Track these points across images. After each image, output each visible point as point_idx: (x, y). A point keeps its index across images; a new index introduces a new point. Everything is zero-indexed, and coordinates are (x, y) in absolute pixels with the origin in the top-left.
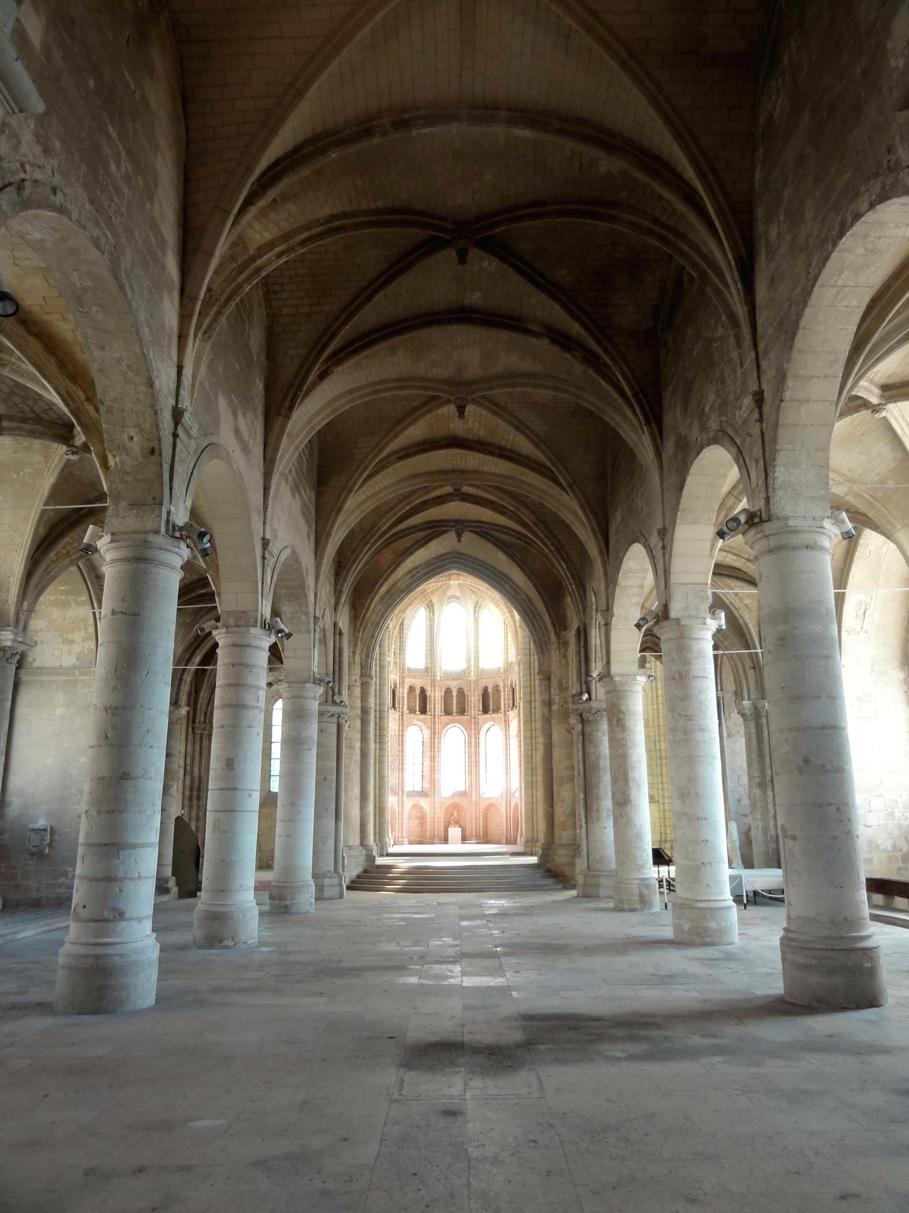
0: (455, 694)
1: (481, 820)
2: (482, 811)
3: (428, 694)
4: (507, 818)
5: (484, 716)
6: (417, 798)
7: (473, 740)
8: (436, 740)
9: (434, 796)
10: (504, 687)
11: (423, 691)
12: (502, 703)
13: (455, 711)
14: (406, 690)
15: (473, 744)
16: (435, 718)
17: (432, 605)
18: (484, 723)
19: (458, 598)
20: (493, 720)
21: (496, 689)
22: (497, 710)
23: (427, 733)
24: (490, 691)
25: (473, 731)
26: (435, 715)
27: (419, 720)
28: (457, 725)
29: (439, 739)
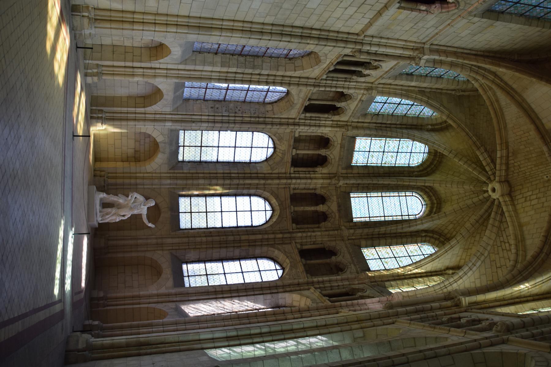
0: (321, 208)
1: (134, 254)
2: (148, 255)
3: (319, 169)
4: (139, 297)
5: (296, 251)
6: (167, 151)
7: (259, 237)
8: (256, 181)
9: (170, 178)
10: (347, 279)
11: (322, 161)
12: (326, 278)
13: (297, 209)
14: (326, 131)
15: (252, 237)
16: (286, 178)
17: (428, 174)
18: (285, 253)
19: (439, 209)
20: (293, 266)
21: (339, 269)
22: (310, 271)
23: (266, 169)
24: (333, 258)
25: (272, 236)
26: (291, 178)
27: (284, 154)
28: (277, 213)
29: (257, 187)
